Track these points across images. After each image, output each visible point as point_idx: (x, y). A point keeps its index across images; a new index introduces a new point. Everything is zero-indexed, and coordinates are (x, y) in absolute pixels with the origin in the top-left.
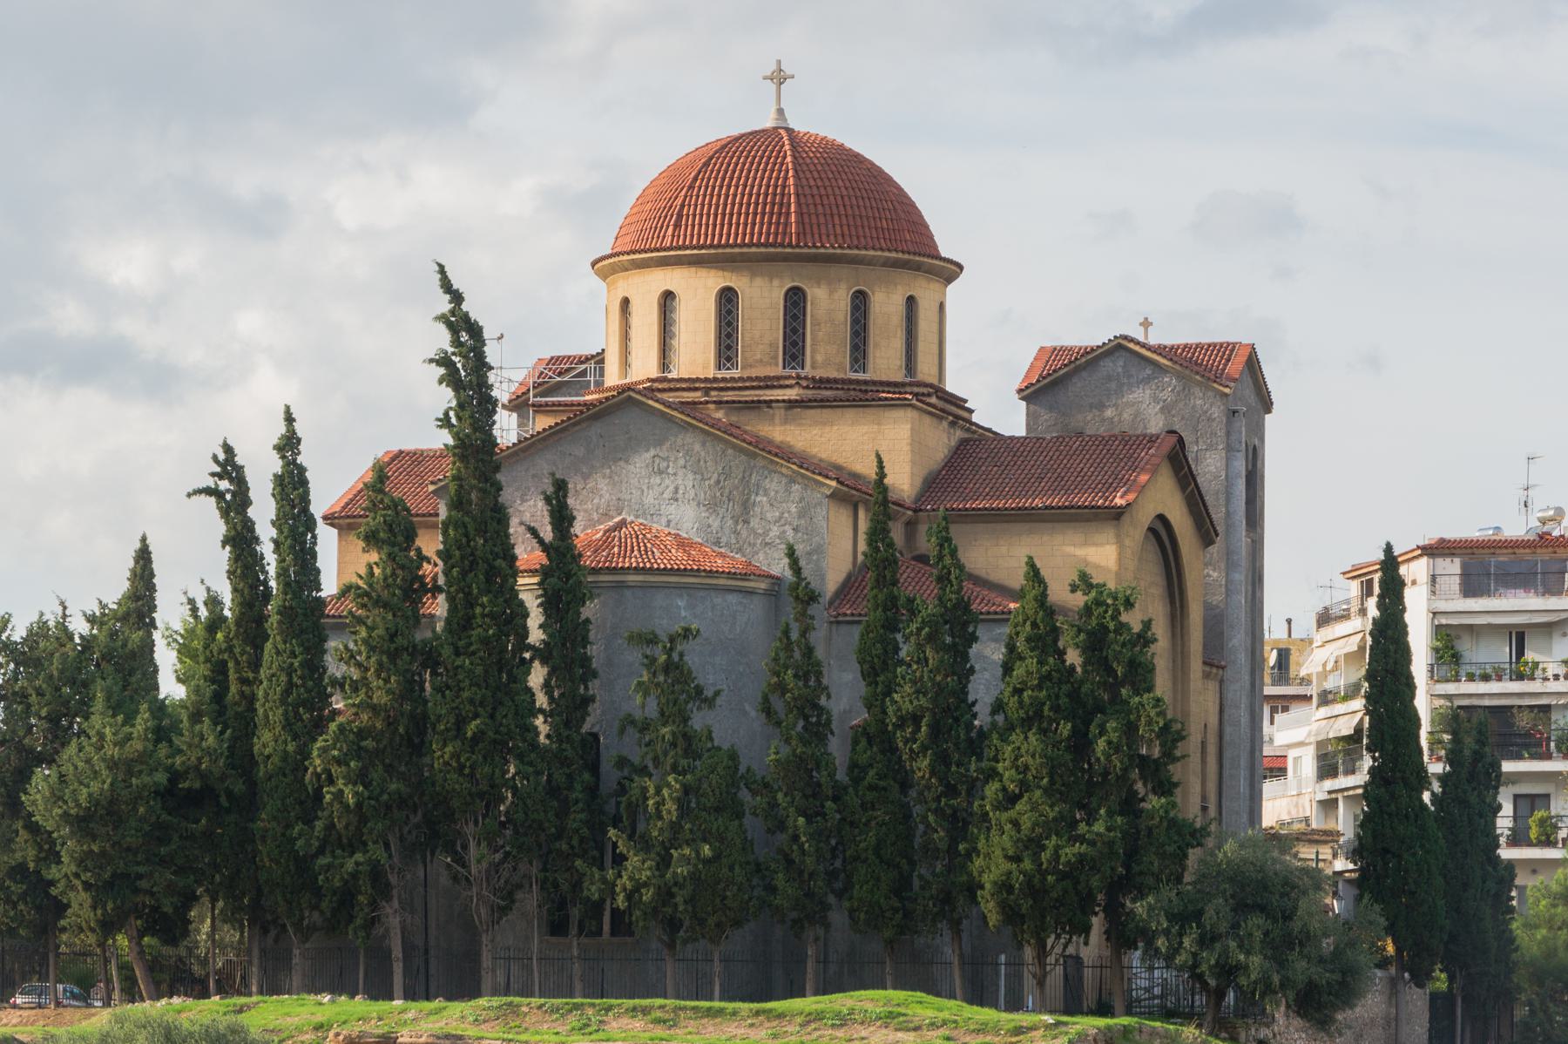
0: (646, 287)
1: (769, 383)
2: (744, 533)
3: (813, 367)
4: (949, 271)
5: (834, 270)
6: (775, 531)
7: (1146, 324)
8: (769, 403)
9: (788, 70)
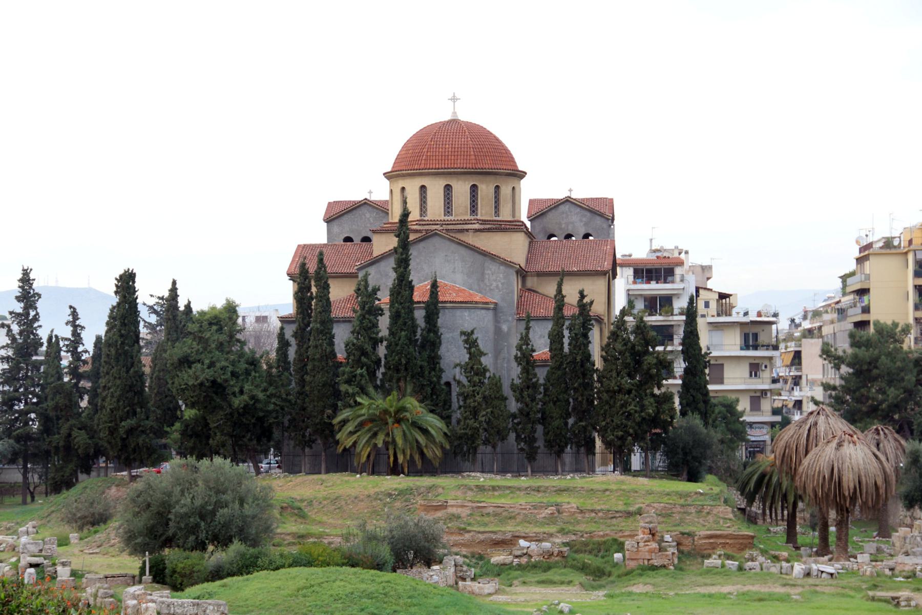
0: (412, 187)
1: (466, 222)
4: (521, 175)
5: (489, 178)
6: (494, 284)
7: (370, 192)
8: (467, 230)
9: (457, 96)
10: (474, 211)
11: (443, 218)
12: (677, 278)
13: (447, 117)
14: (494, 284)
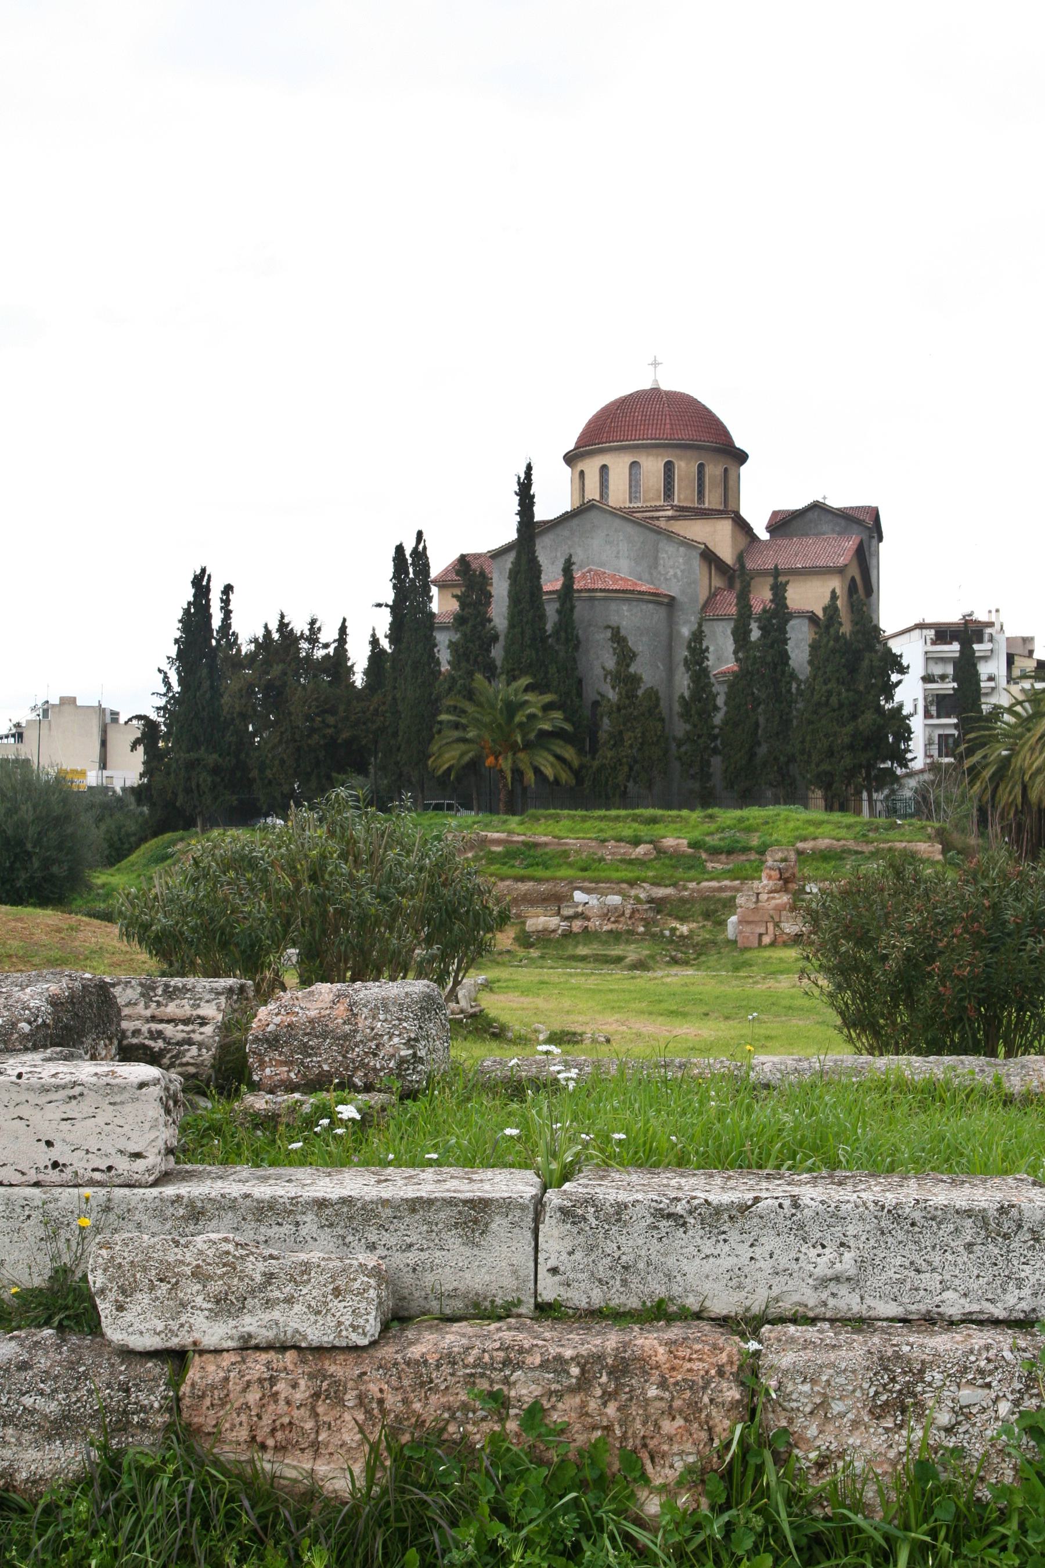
1: (657, 509)
2: (655, 574)
3: (679, 501)
4: (741, 457)
6: (671, 572)
9: (659, 360)
10: (669, 496)
11: (627, 505)
12: (986, 637)
13: (647, 386)
14: (671, 572)
